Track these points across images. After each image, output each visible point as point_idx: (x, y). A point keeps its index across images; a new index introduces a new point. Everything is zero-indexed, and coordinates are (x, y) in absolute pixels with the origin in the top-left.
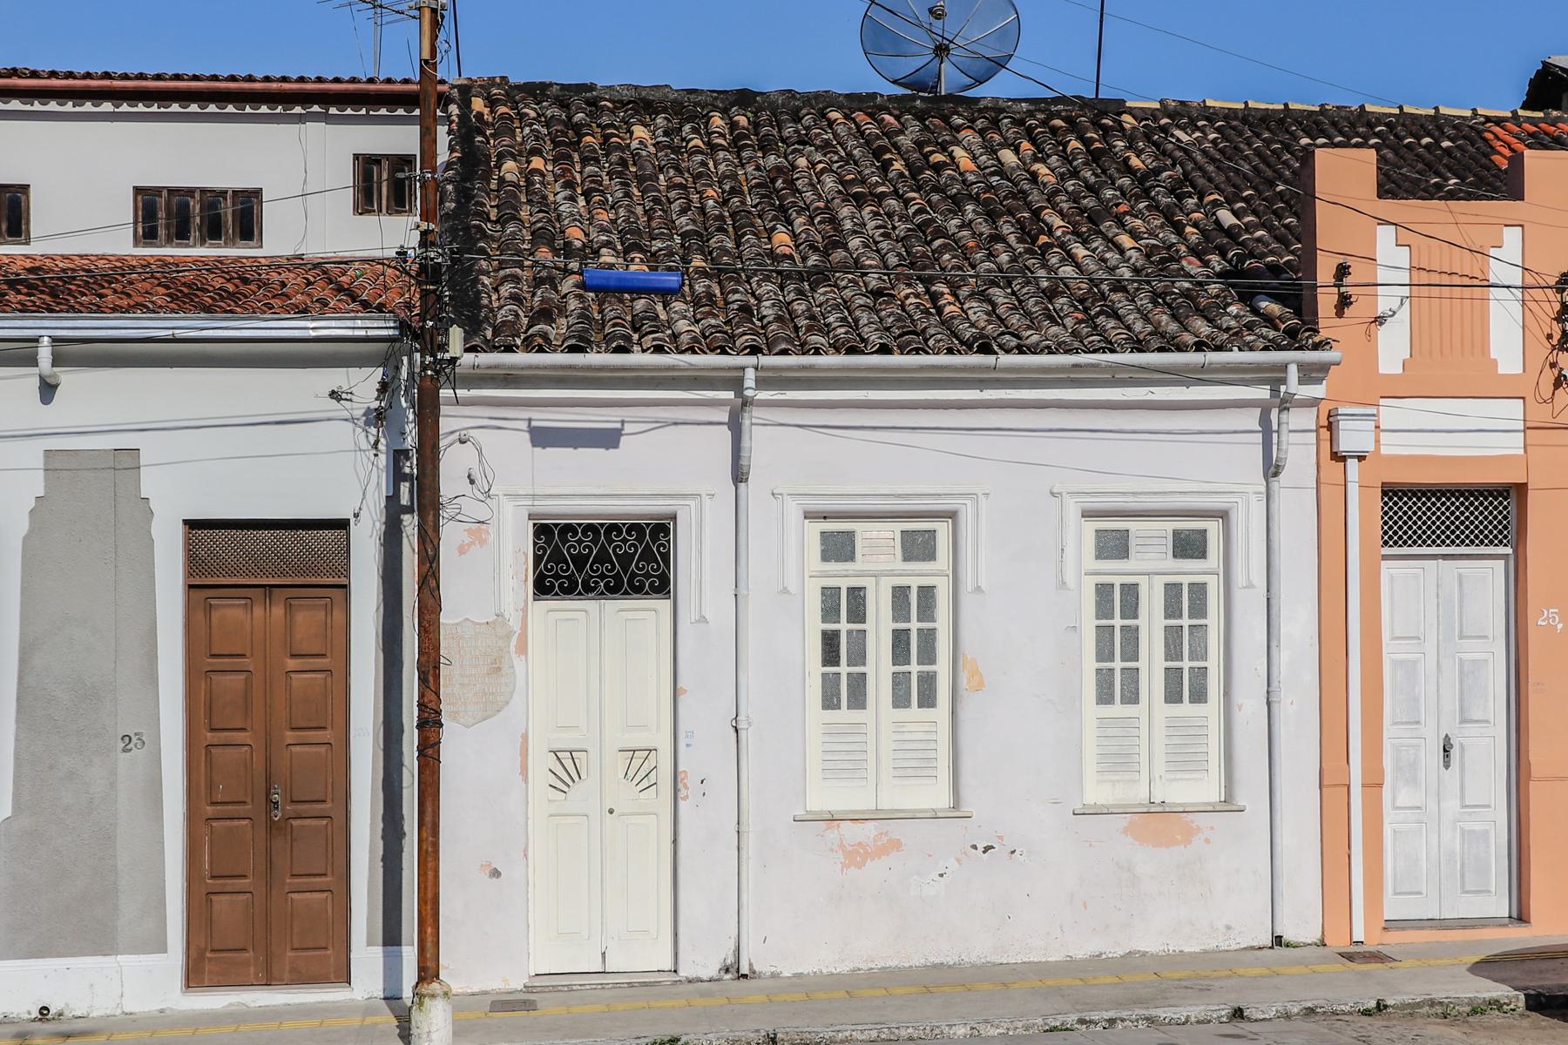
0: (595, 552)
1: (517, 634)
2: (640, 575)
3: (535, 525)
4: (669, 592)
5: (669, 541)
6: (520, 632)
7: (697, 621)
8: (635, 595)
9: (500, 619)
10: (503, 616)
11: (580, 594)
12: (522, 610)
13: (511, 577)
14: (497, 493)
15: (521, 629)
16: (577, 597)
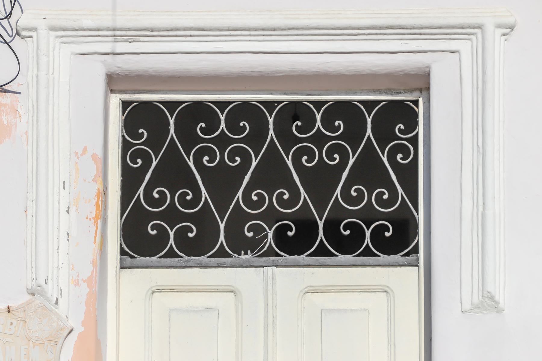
0: (254, 164)
1: (74, 336)
2: (352, 214)
3: (125, 104)
4: (416, 250)
5: (414, 141)
6: (82, 329)
7: (477, 308)
8: (341, 258)
9: (38, 300)
10: (43, 294)
11: (221, 253)
12: (89, 281)
13: (64, 209)
14: (32, 23)
15: (83, 323)
16: (214, 260)
